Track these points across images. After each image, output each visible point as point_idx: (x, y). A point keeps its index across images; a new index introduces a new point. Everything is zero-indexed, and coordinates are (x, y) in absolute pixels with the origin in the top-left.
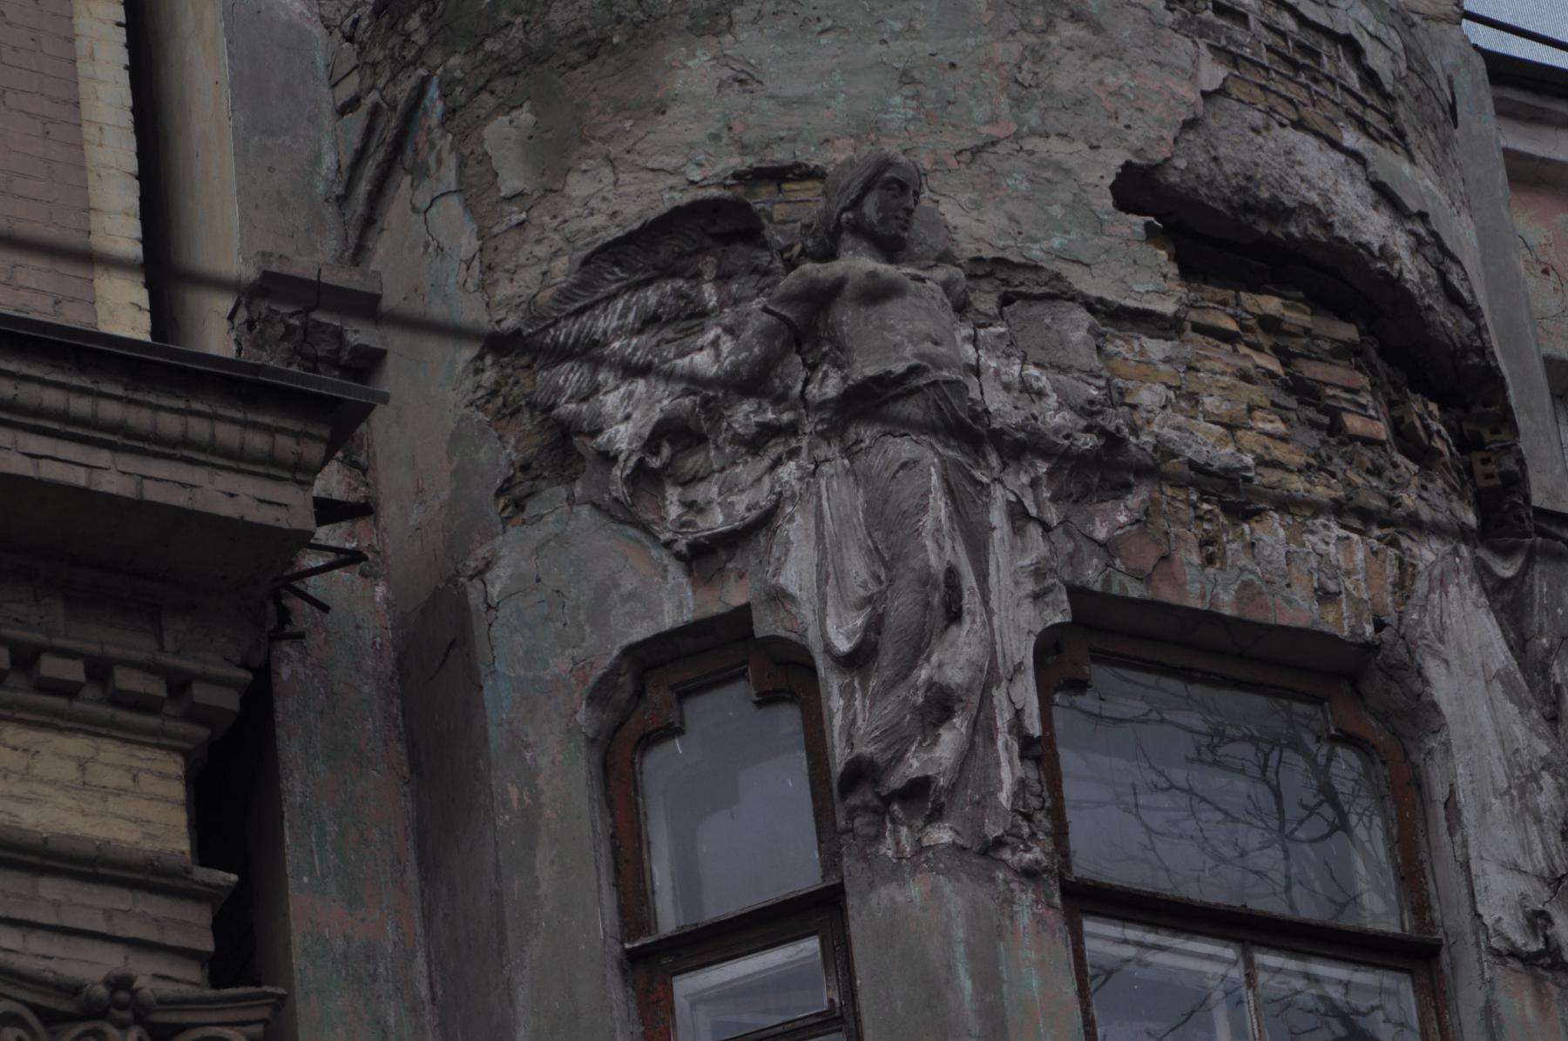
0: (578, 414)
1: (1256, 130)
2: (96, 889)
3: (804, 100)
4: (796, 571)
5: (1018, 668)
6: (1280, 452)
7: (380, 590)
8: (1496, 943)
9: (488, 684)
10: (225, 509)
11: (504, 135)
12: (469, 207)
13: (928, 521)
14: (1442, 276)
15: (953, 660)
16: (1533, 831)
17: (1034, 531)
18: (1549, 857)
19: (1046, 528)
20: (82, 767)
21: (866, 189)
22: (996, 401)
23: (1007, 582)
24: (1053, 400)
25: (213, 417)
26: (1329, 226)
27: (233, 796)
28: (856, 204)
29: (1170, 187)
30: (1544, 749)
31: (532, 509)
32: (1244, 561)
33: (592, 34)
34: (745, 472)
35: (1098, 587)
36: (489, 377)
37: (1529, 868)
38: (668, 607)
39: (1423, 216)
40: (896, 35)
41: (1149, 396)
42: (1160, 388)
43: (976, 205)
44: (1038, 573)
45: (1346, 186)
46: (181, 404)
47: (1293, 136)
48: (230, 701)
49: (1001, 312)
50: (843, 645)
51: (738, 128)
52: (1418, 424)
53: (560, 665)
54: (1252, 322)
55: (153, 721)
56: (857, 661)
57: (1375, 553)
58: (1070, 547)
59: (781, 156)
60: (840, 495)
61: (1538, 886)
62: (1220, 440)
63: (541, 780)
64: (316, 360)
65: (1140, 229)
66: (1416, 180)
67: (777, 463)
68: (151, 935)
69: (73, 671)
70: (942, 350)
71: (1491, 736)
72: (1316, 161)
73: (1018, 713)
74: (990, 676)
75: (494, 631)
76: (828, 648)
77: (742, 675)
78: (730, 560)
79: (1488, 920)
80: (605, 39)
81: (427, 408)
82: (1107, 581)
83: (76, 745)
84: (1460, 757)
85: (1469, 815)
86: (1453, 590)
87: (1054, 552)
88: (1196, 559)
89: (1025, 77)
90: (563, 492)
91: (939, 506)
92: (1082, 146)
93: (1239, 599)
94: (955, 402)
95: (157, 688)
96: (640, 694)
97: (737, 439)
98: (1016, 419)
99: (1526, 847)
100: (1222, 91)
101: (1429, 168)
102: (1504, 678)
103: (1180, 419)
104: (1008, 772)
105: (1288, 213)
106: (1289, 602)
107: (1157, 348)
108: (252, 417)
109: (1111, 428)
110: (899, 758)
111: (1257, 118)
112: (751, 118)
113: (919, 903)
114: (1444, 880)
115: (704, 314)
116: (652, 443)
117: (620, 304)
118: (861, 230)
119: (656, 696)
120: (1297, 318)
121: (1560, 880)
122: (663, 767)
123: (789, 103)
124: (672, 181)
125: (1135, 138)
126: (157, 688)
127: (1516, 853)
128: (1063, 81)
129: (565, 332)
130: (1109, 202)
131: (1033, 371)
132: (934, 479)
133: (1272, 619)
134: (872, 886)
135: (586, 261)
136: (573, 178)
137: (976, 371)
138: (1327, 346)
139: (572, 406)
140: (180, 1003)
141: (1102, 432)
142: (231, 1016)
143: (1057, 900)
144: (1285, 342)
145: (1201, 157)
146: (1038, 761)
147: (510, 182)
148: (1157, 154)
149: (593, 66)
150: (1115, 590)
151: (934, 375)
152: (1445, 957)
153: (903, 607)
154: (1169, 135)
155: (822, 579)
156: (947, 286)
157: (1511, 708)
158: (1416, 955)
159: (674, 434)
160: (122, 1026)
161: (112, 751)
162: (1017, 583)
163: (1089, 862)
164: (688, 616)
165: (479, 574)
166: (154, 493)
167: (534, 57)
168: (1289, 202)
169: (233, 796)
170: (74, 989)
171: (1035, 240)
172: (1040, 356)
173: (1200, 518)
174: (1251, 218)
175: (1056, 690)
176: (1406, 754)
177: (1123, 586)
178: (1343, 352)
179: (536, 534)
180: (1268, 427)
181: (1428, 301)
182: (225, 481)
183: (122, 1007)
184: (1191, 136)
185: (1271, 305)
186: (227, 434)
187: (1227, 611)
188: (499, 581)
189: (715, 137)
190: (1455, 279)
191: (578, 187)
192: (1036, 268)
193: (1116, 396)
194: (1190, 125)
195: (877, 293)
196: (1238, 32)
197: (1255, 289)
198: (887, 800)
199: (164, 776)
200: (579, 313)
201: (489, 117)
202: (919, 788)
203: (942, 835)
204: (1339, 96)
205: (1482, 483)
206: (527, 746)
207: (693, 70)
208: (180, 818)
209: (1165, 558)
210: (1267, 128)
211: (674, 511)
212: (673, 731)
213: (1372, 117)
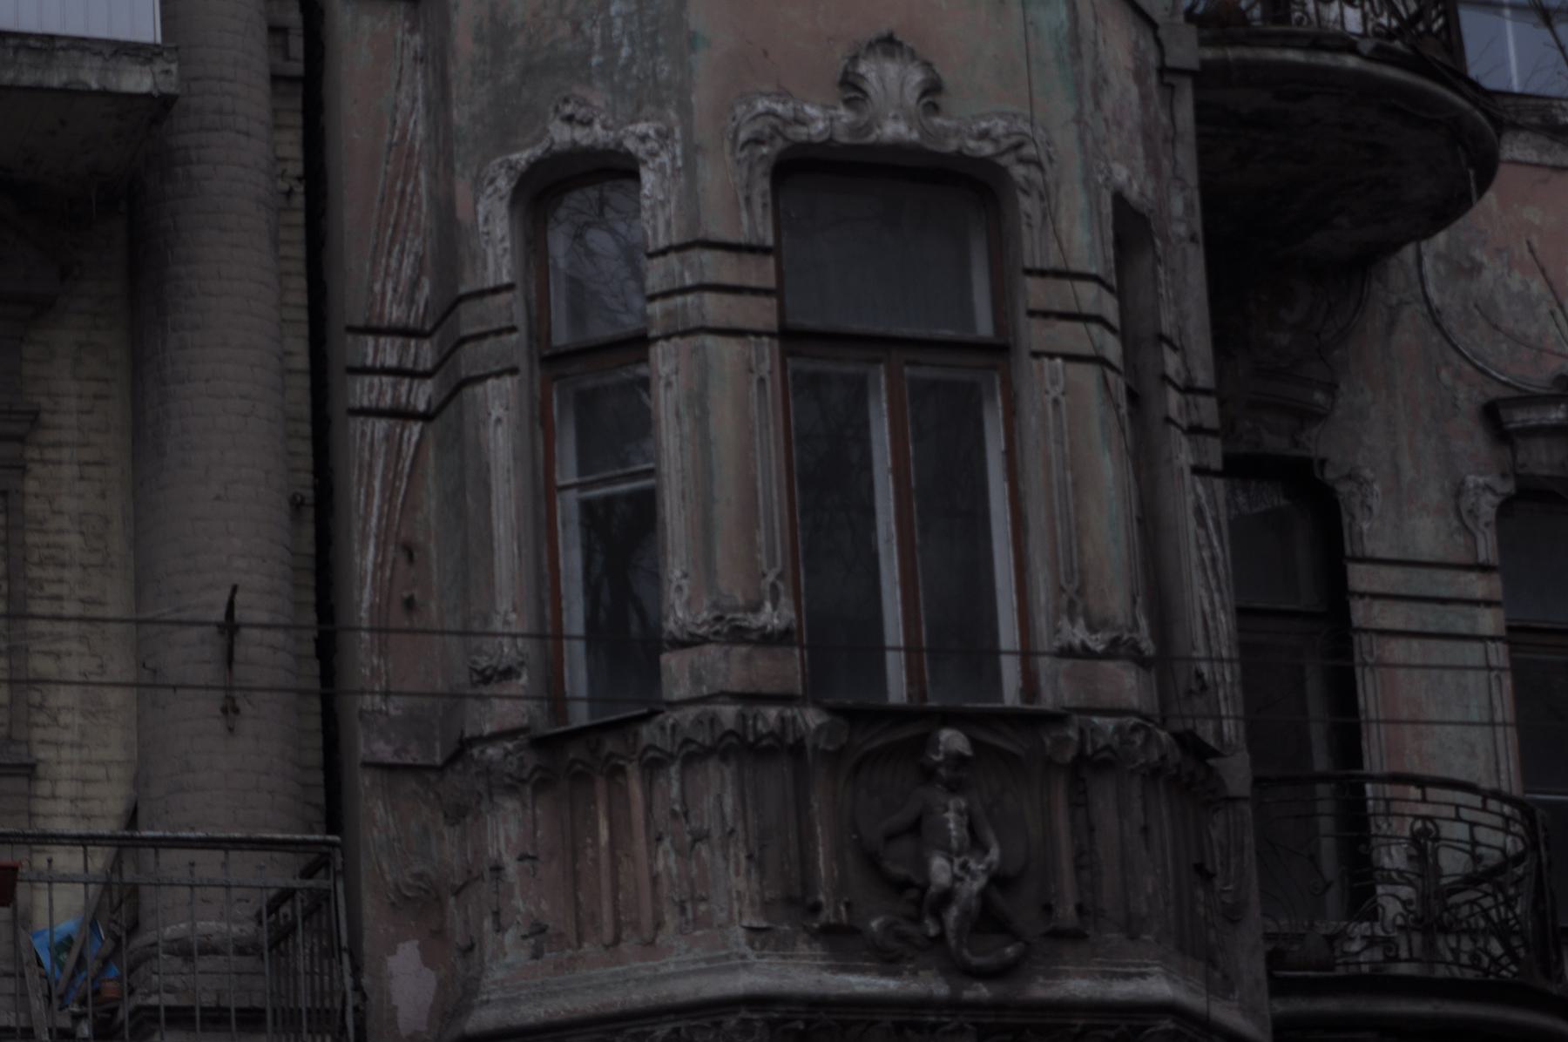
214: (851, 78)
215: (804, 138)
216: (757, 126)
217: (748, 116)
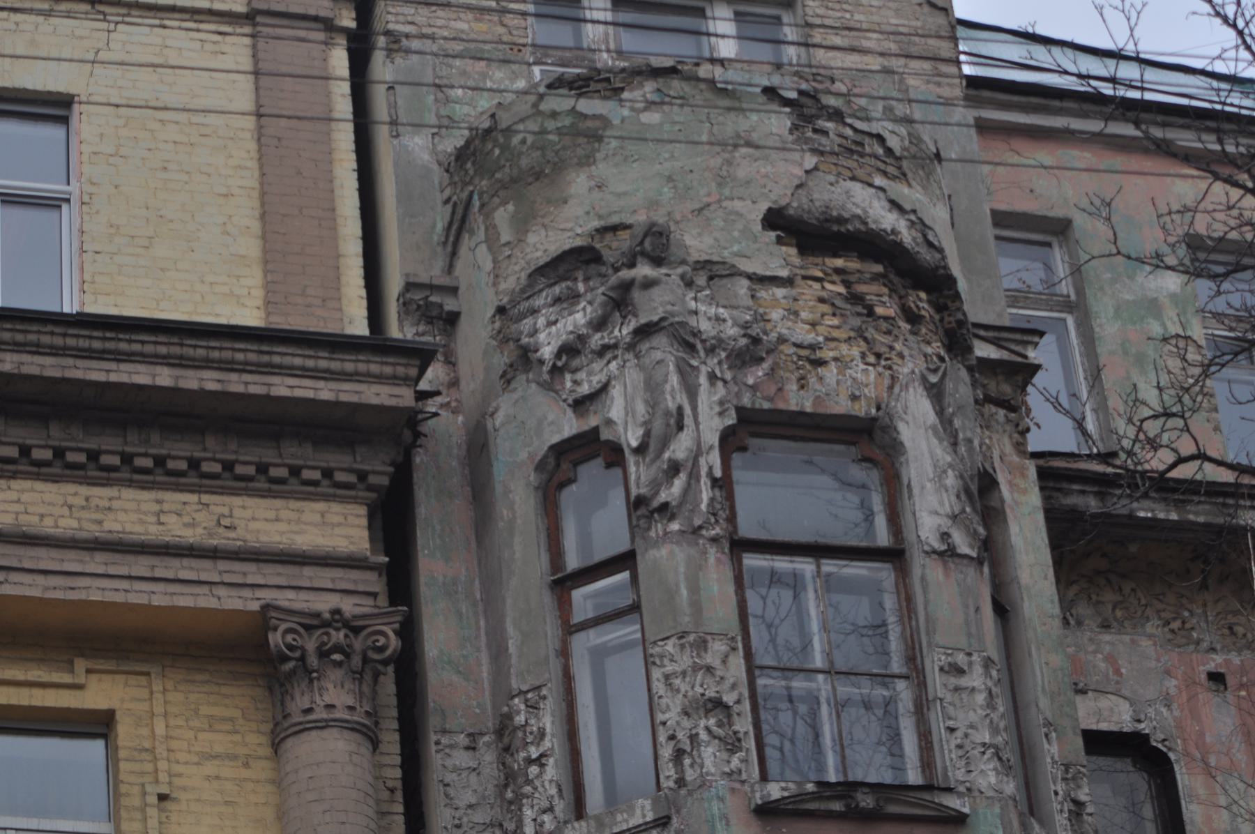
0: (529, 343)
1: (832, 184)
2: (327, 569)
3: (625, 194)
4: (616, 411)
5: (711, 447)
6: (836, 334)
7: (460, 418)
8: (926, 548)
9: (495, 464)
10: (375, 401)
11: (503, 216)
12: (490, 248)
13: (668, 387)
14: (925, 236)
15: (680, 448)
16: (945, 495)
17: (720, 384)
18: (951, 506)
19: (725, 382)
20: (323, 516)
21: (645, 236)
22: (705, 326)
23: (707, 409)
24: (730, 323)
25: (368, 362)
26: (866, 224)
27: (394, 520)
28: (641, 243)
29: (790, 216)
30: (949, 459)
31: (513, 385)
32: (818, 387)
33: (537, 169)
34: (596, 366)
35: (749, 406)
36: (497, 325)
37: (942, 512)
38: (567, 428)
39: (914, 211)
40: (666, 160)
41: (776, 315)
42: (781, 311)
43: (700, 235)
44: (721, 403)
45: (876, 204)
46: (353, 358)
47: (850, 184)
48: (385, 481)
49: (709, 285)
50: (634, 444)
51: (597, 208)
53: (523, 455)
54: (830, 271)
55: (353, 493)
56: (640, 450)
57: (880, 374)
58: (736, 389)
59: (615, 220)
60: (633, 376)
61: (946, 520)
62: (808, 332)
63: (516, 507)
65: (774, 239)
66: (910, 194)
67: (609, 362)
68: (351, 587)
69: (316, 475)
70: (676, 308)
71: (927, 455)
72: (860, 194)
73: (711, 468)
74: (698, 452)
75: (498, 441)
76: (629, 445)
79: (923, 538)
80: (542, 171)
81: (475, 340)
82: (753, 403)
83: (320, 506)
84: (913, 466)
85: (916, 491)
86: (911, 390)
87: (728, 393)
88: (795, 387)
89: (724, 173)
90: (524, 377)
91: (674, 379)
92: (749, 202)
93: (814, 404)
94: (681, 331)
95: (352, 478)
96: (558, 465)
97: (593, 352)
98: (713, 333)
99: (941, 503)
100: (816, 168)
101: (919, 188)
102: (934, 428)
103: (790, 324)
104: (706, 494)
105: (846, 221)
106: (837, 403)
107: (780, 292)
108: (385, 360)
109: (754, 334)
110: (657, 493)
111: (832, 178)
112: (603, 203)
113: (667, 558)
114: (907, 520)
116: (558, 355)
117: (544, 294)
118: (644, 254)
119: (565, 466)
121: (956, 517)
122: (568, 496)
123: (619, 195)
124: (569, 234)
125: (773, 197)
126: (352, 478)
127: (936, 506)
128: (741, 173)
129: (524, 306)
130: (760, 227)
131: (721, 310)
132: (672, 368)
133: (829, 412)
134: (646, 550)
135: (530, 276)
136: (530, 235)
137: (696, 313)
138: (868, 276)
139: (527, 340)
140: (364, 617)
141: (750, 336)
142: (386, 620)
143: (727, 550)
144: (845, 277)
145: (804, 200)
146: (721, 487)
147: (506, 236)
148: (783, 202)
149: (537, 184)
150: (757, 406)
151: (672, 320)
152: (907, 554)
153: (658, 426)
154: (789, 192)
155: (627, 415)
156: (682, 277)
157: (935, 441)
158: (895, 555)
159: (569, 350)
160: (337, 629)
161: (336, 507)
162: (711, 408)
163: (748, 528)
164: (574, 432)
165: (492, 415)
166: (344, 398)
167: (514, 181)
168: (846, 215)
169: (394, 520)
170: (317, 615)
171: (726, 248)
172: (723, 302)
173: (798, 368)
174: (828, 225)
176: (893, 464)
178: (875, 278)
179: (515, 396)
180: (830, 323)
181: (917, 249)
182: (375, 388)
183: (337, 621)
184: (800, 191)
185: (839, 263)
186: (374, 368)
187: (809, 410)
188: (500, 418)
189: (588, 213)
190: (931, 238)
191: (532, 238)
192: (724, 263)
194: (799, 186)
195: (649, 284)
196: (824, 140)
197: (835, 255)
198: (652, 512)
199: (358, 516)
200: (528, 298)
201: (497, 208)
202: (664, 507)
203: (675, 526)
204: (873, 161)
205: (947, 326)
206: (511, 491)
207: (579, 183)
208: (366, 534)
209: (780, 390)
210: (837, 182)
211: (568, 384)
212: (571, 481)
213: (891, 169)
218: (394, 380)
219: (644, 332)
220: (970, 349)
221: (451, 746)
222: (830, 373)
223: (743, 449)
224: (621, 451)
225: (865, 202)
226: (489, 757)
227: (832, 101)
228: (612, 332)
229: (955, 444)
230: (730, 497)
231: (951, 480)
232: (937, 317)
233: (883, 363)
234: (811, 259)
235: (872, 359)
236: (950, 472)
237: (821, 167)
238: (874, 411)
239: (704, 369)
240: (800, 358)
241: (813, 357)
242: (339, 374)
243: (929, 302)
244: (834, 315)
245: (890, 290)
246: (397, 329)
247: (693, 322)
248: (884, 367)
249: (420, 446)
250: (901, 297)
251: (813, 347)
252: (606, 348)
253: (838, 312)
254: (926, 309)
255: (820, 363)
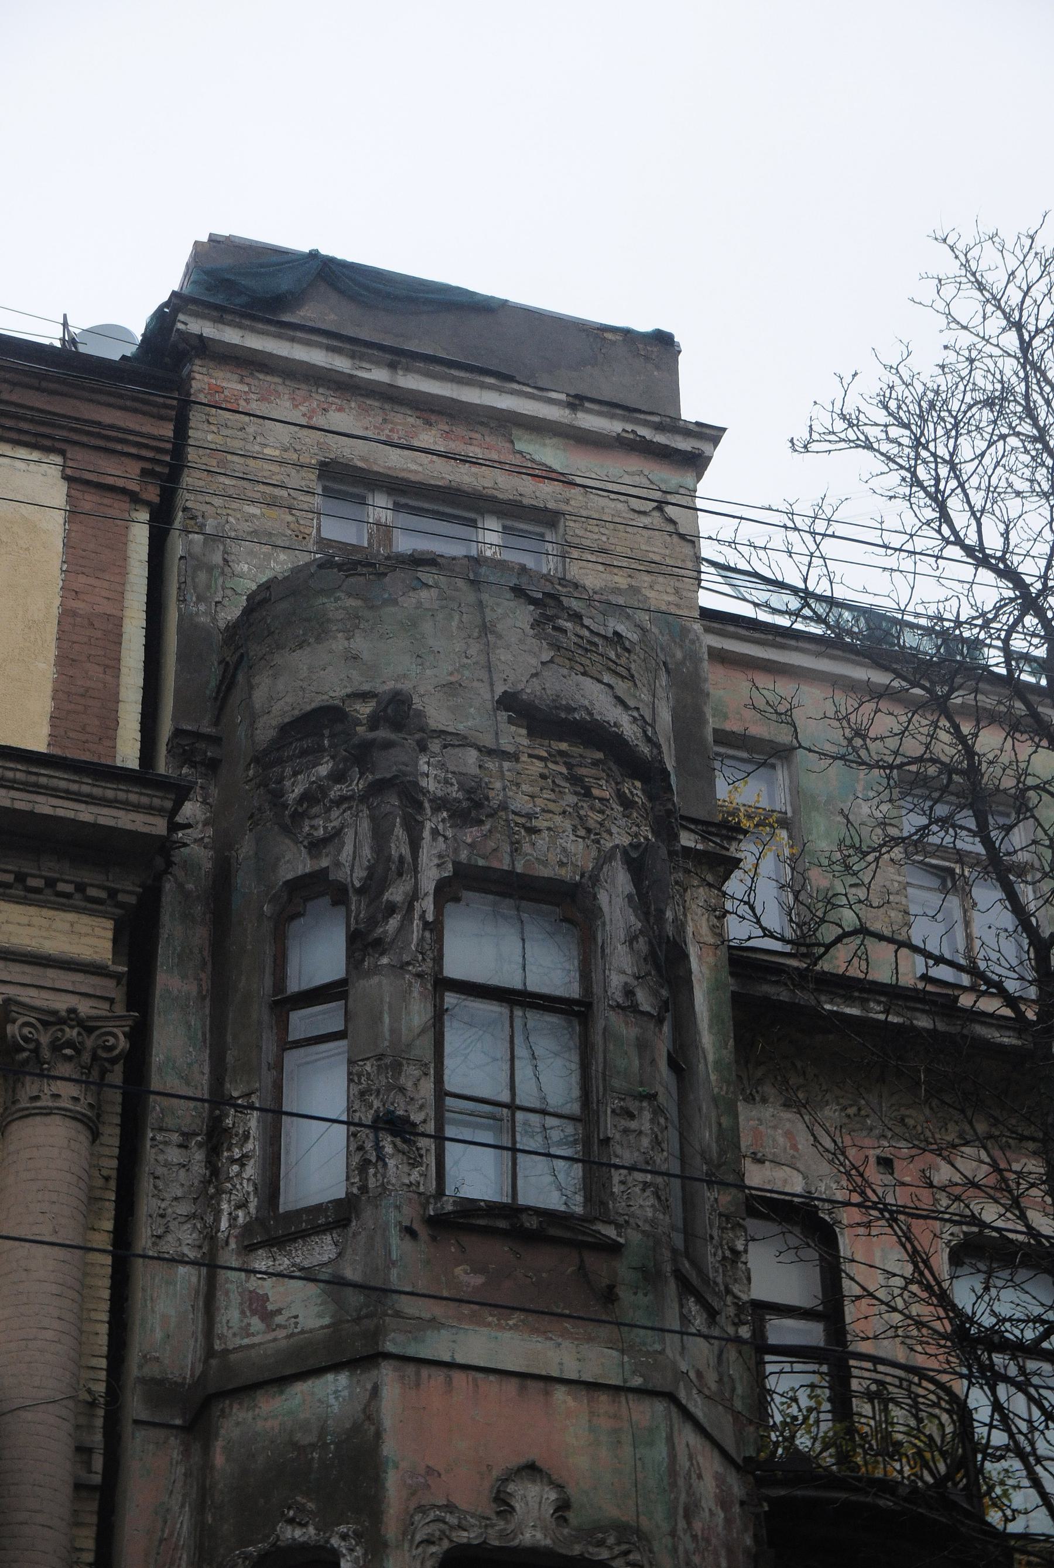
1: (564, 677)
2: (70, 973)
5: (426, 894)
6: (551, 806)
10: (129, 826)
14: (645, 732)
17: (441, 839)
19: (446, 838)
20: (72, 925)
24: (456, 788)
25: (127, 791)
26: (591, 714)
28: (385, 710)
30: (639, 925)
32: (530, 851)
35: (465, 862)
38: (300, 867)
45: (602, 697)
46: (115, 786)
47: (580, 678)
48: (132, 900)
50: (357, 884)
52: (627, 791)
55: (101, 908)
60: (365, 826)
64: (196, 763)
65: (505, 718)
67: (344, 811)
68: (91, 991)
69: (69, 888)
73: (424, 912)
76: (353, 885)
77: (327, 894)
78: (325, 848)
82: (469, 859)
83: (71, 916)
95: (103, 895)
97: (331, 801)
100: (551, 661)
108: (144, 791)
114: (596, 977)
115: (325, 750)
120: (577, 750)
126: (103, 895)
142: (118, 1023)
145: (538, 688)
146: (431, 931)
148: (520, 687)
150: (473, 862)
152: (595, 1006)
160: (72, 1027)
161: (85, 919)
163: (453, 969)
166: (101, 821)
170: (55, 1013)
175: (447, 901)
177: (476, 860)
178: (595, 763)
181: (636, 742)
183: (72, 1020)
185: (564, 746)
186: (133, 798)
193: (484, 785)
194: (535, 675)
195: (388, 745)
196: (561, 637)
197: (561, 740)
199: (104, 929)
203: (385, 960)
208: (109, 945)
212: (299, 915)
214: (502, 1496)
215: (465, 1540)
216: (428, 1530)
217: (423, 1523)
218: (149, 810)
219: (379, 787)
220: (676, 837)
221: (166, 1143)
222: (542, 841)
223: (457, 900)
224: (347, 891)
225: (595, 698)
226: (199, 1156)
227: (575, 605)
228: (350, 785)
229: (647, 914)
230: (439, 941)
231: (642, 945)
232: (649, 805)
233: (592, 837)
234: (538, 741)
235: (582, 832)
236: (641, 939)
237: (556, 660)
238: (578, 878)
239: (428, 825)
240: (517, 824)
241: (528, 825)
242: (100, 799)
243: (643, 790)
244: (553, 790)
245: (608, 775)
246: (163, 766)
247: (423, 783)
248: (593, 841)
249: (171, 873)
250: (617, 783)
251: (529, 816)
252: (343, 799)
253: (557, 789)
254: (640, 797)
255: (536, 831)
